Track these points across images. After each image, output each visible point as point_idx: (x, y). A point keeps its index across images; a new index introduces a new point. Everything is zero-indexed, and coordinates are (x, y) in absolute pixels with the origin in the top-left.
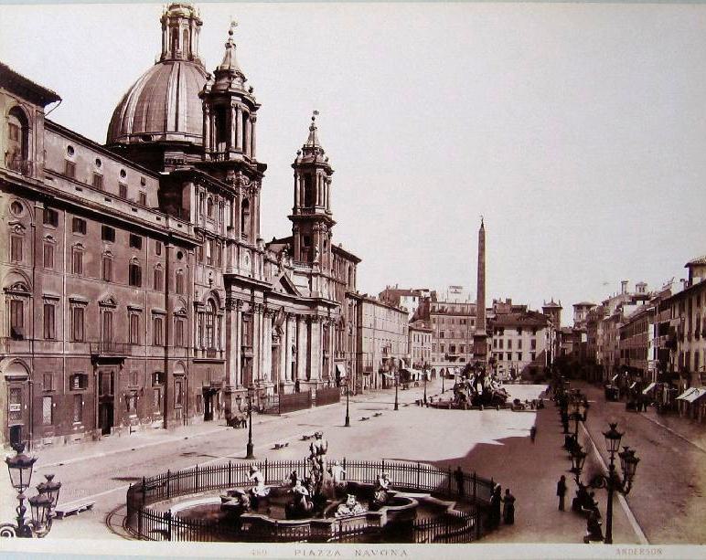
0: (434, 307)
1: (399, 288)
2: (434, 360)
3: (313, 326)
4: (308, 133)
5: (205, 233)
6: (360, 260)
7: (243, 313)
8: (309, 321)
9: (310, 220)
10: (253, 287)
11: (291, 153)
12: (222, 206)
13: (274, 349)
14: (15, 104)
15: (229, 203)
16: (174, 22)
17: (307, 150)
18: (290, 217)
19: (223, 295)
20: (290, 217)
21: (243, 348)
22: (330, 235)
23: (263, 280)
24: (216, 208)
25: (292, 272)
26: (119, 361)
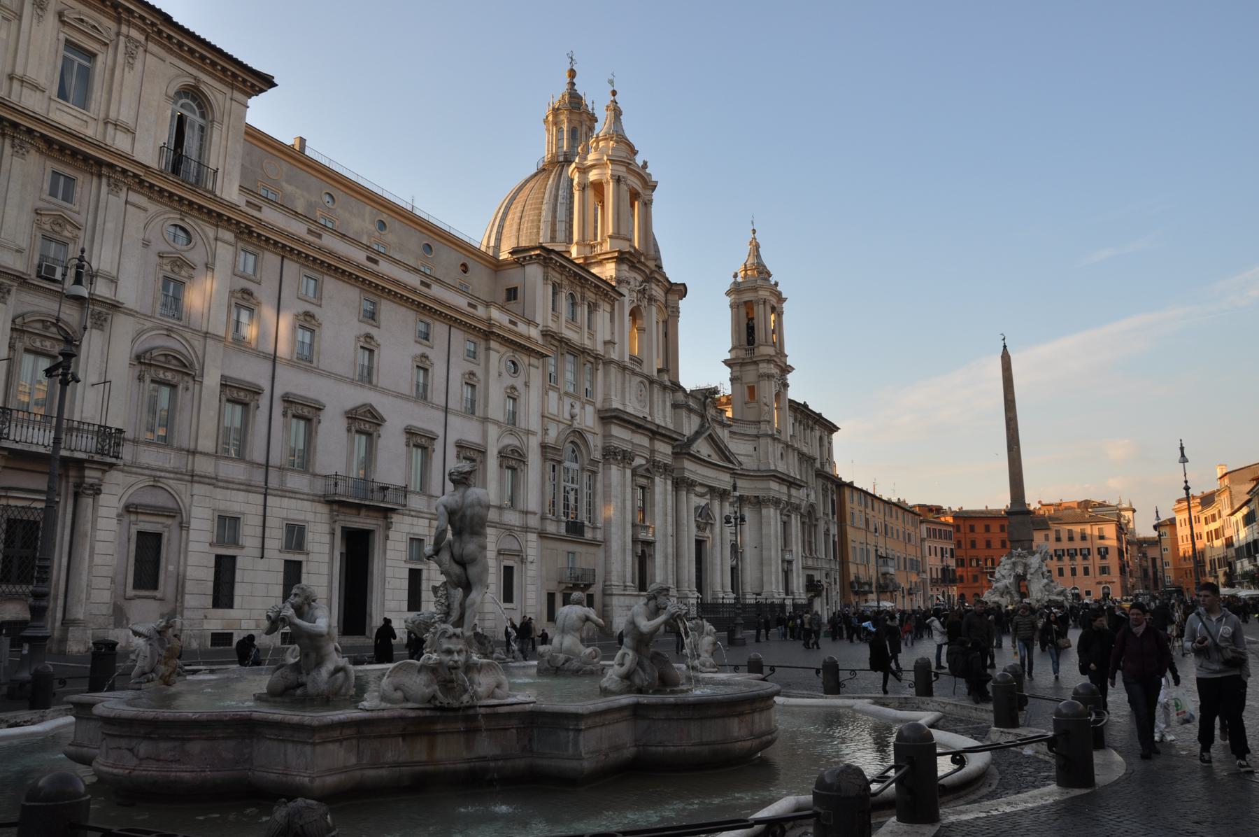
5: (563, 342)
7: (634, 473)
8: (759, 503)
10: (655, 433)
12: (593, 308)
13: (700, 543)
14: (191, 81)
15: (608, 308)
18: (726, 362)
19: (596, 443)
20: (726, 362)
21: (634, 525)
22: (786, 386)
23: (671, 426)
24: (582, 312)
25: (726, 432)
26: (386, 513)
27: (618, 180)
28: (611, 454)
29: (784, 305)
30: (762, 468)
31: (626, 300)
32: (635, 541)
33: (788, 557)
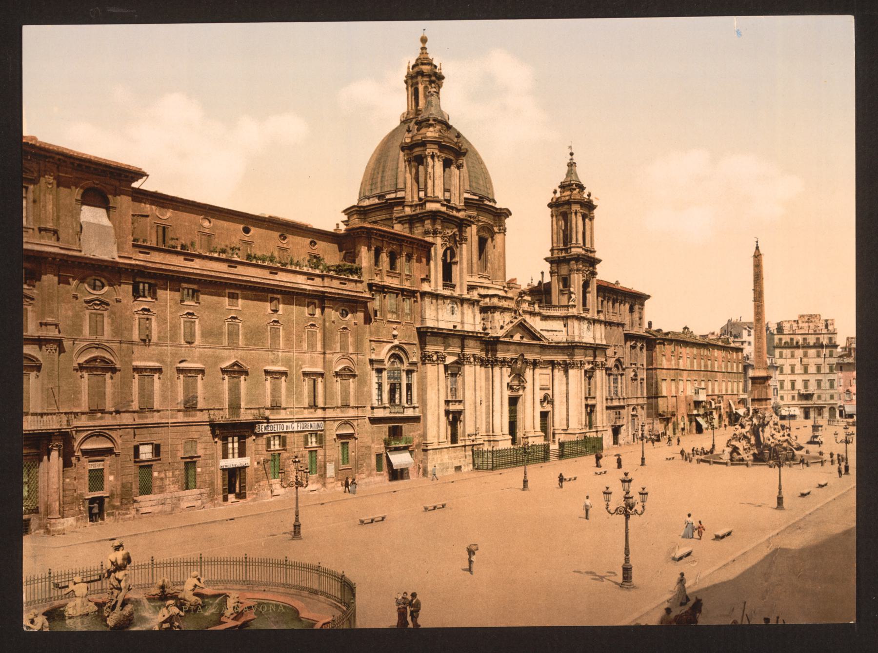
0: (780, 340)
1: (743, 320)
2: (782, 398)
3: (571, 372)
4: (566, 169)
6: (649, 297)
9: (571, 258)
11: (548, 189)
16: (414, 81)
17: (563, 187)
18: (546, 259)
20: (546, 259)
27: (433, 157)
28: (425, 358)
29: (595, 211)
30: (570, 339)
31: (439, 246)
32: (447, 413)
33: (590, 402)
